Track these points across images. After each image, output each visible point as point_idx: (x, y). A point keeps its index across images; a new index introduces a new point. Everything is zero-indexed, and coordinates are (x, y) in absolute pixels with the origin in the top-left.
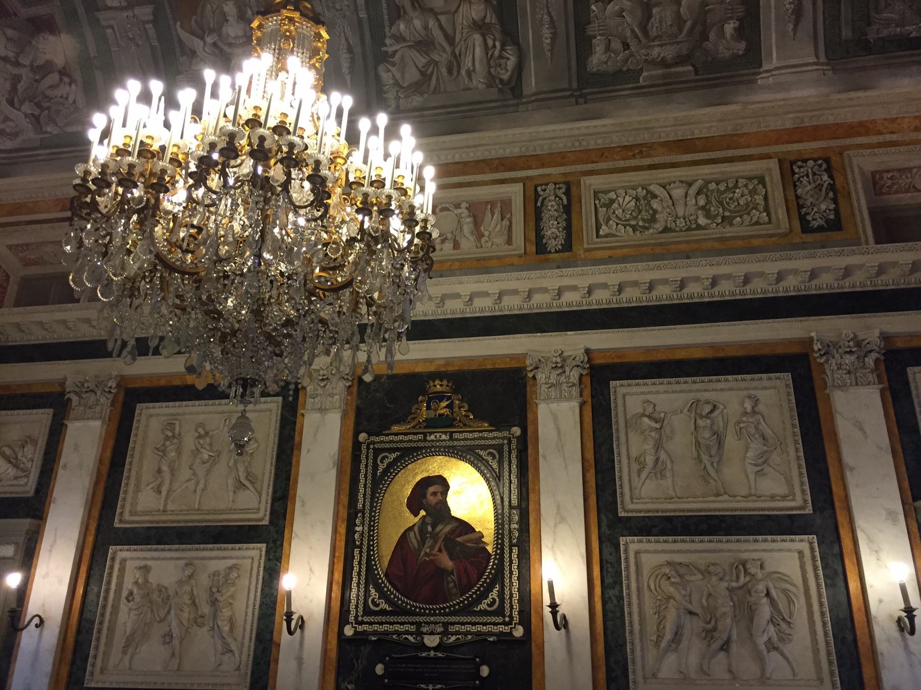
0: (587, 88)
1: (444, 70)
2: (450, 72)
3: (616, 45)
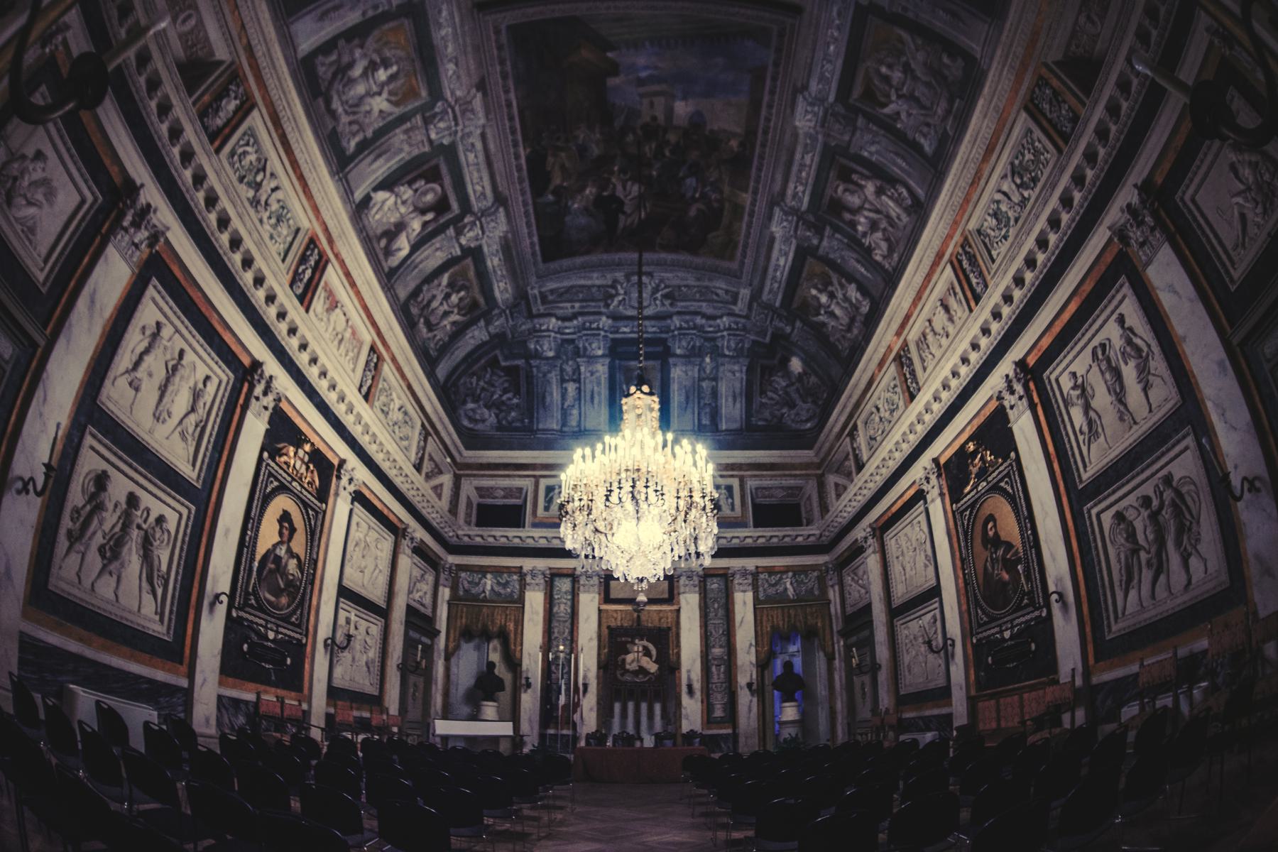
0: (936, 167)
1: (890, 229)
2: (892, 226)
3: (925, 130)
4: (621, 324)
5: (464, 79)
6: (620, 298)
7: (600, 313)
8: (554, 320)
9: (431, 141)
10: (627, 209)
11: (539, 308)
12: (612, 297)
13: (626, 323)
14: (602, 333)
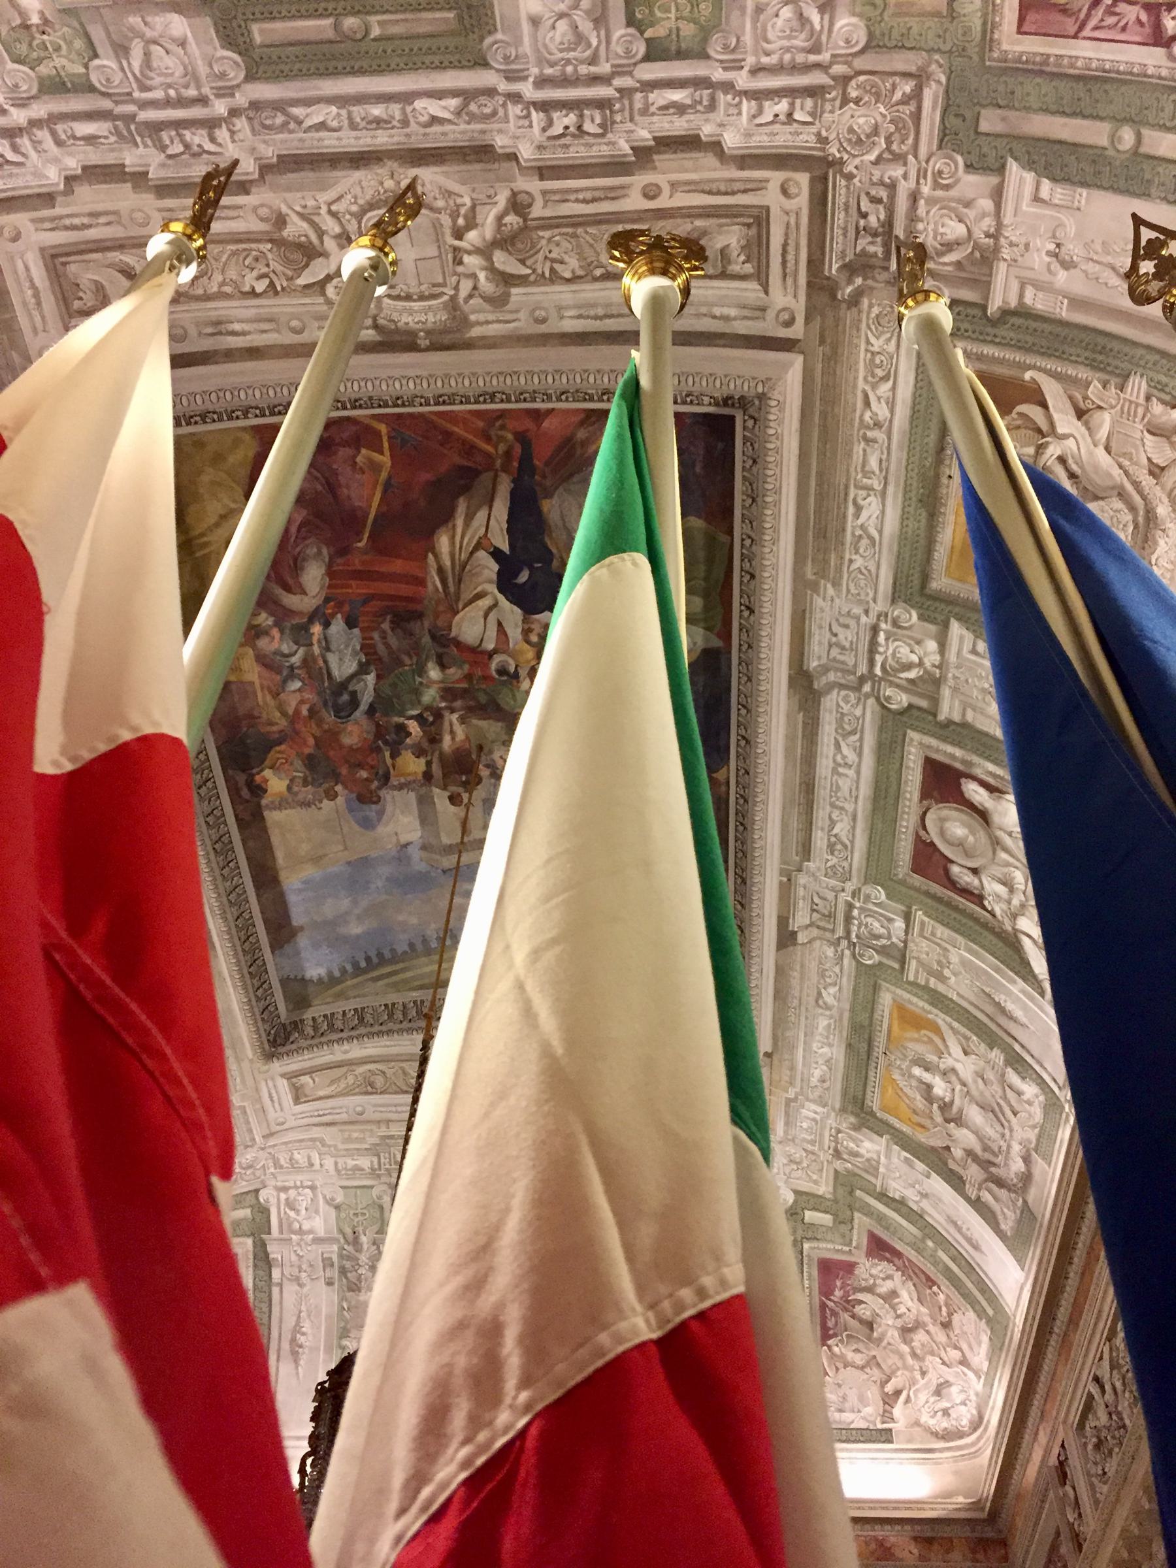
4: (458, 133)
5: (813, 966)
6: (472, 236)
7: (544, 172)
8: (731, 140)
9: (908, 918)
10: (492, 567)
11: (785, 200)
12: (504, 241)
13: (437, 138)
14: (527, 90)
